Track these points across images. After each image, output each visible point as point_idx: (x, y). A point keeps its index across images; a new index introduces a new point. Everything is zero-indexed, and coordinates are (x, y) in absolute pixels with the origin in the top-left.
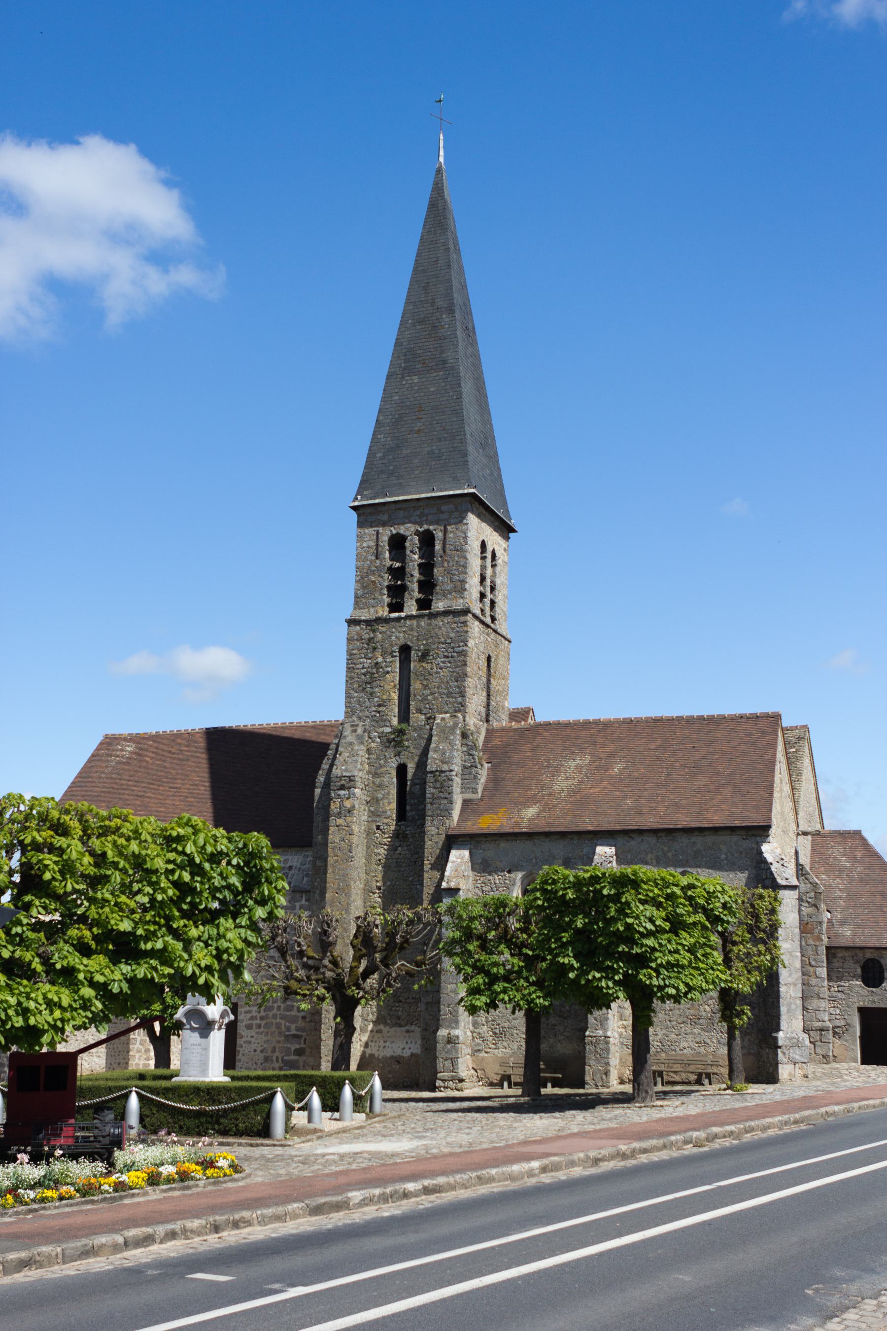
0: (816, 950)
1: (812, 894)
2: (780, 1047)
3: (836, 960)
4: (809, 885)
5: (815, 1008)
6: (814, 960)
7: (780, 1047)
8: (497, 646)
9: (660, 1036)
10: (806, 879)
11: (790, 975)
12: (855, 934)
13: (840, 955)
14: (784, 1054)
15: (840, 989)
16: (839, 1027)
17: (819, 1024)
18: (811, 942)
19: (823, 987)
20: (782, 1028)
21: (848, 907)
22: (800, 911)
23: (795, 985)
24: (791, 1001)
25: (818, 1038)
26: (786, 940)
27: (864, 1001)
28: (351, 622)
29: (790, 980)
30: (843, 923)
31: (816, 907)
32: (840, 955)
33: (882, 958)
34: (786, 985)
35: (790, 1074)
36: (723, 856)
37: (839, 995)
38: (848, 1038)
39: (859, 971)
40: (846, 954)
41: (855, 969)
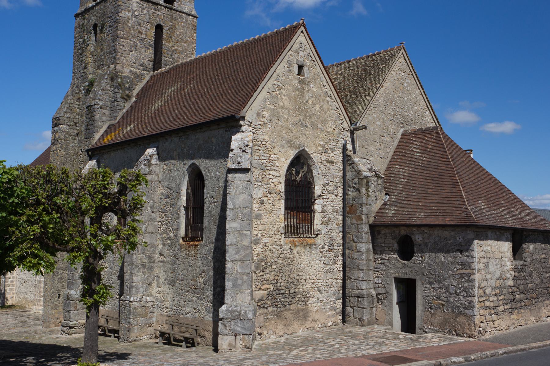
0: (358, 228)
1: (356, 181)
2: (221, 319)
3: (380, 237)
4: (355, 173)
5: (356, 278)
6: (356, 237)
7: (221, 319)
8: (173, 19)
9: (176, 302)
10: (353, 167)
11: (237, 253)
12: (396, 213)
13: (383, 232)
14: (225, 326)
15: (383, 261)
16: (380, 294)
17: (357, 292)
18: (354, 221)
19: (362, 260)
20: (226, 301)
21: (402, 191)
22: (344, 194)
23: (243, 261)
24: (238, 276)
25: (356, 304)
26: (234, 220)
27: (399, 272)
28: (77, 16)
29: (237, 257)
30: (393, 204)
31: (359, 191)
32: (383, 232)
33: (413, 234)
34: (232, 261)
35: (230, 345)
36: (214, 148)
37: (382, 266)
38: (387, 304)
39: (396, 246)
40: (387, 231)
41: (393, 244)
